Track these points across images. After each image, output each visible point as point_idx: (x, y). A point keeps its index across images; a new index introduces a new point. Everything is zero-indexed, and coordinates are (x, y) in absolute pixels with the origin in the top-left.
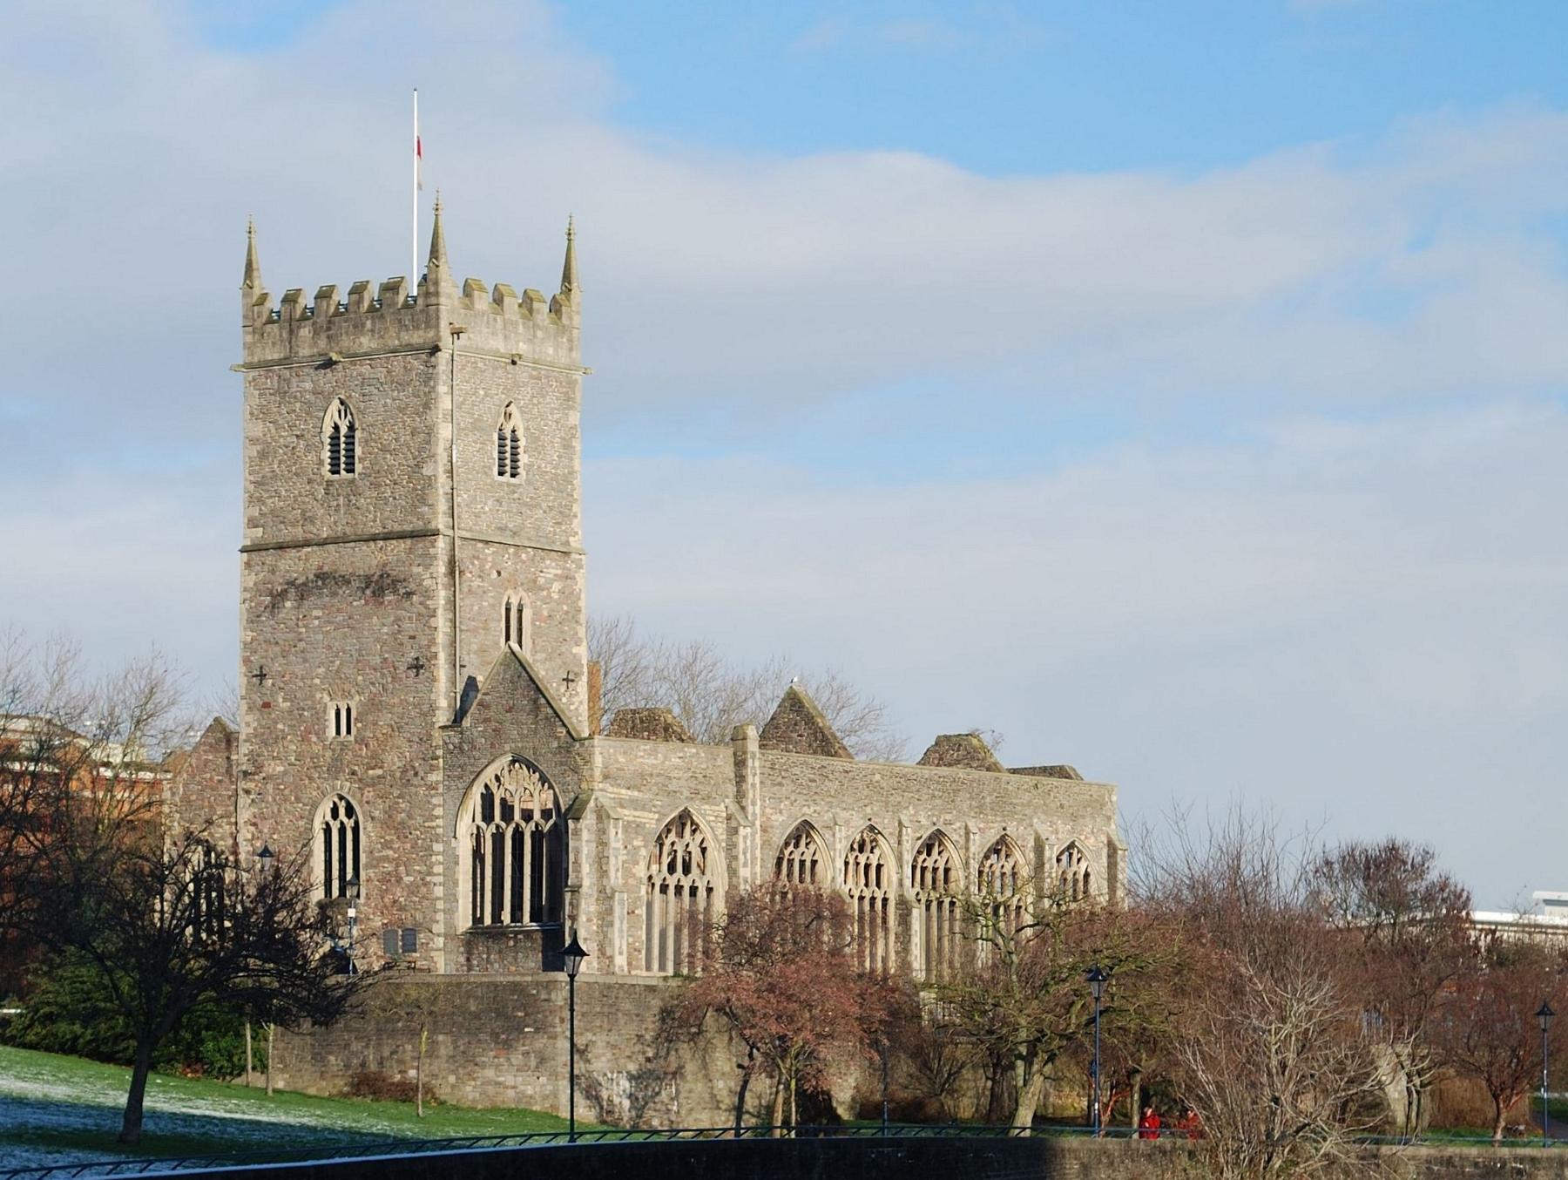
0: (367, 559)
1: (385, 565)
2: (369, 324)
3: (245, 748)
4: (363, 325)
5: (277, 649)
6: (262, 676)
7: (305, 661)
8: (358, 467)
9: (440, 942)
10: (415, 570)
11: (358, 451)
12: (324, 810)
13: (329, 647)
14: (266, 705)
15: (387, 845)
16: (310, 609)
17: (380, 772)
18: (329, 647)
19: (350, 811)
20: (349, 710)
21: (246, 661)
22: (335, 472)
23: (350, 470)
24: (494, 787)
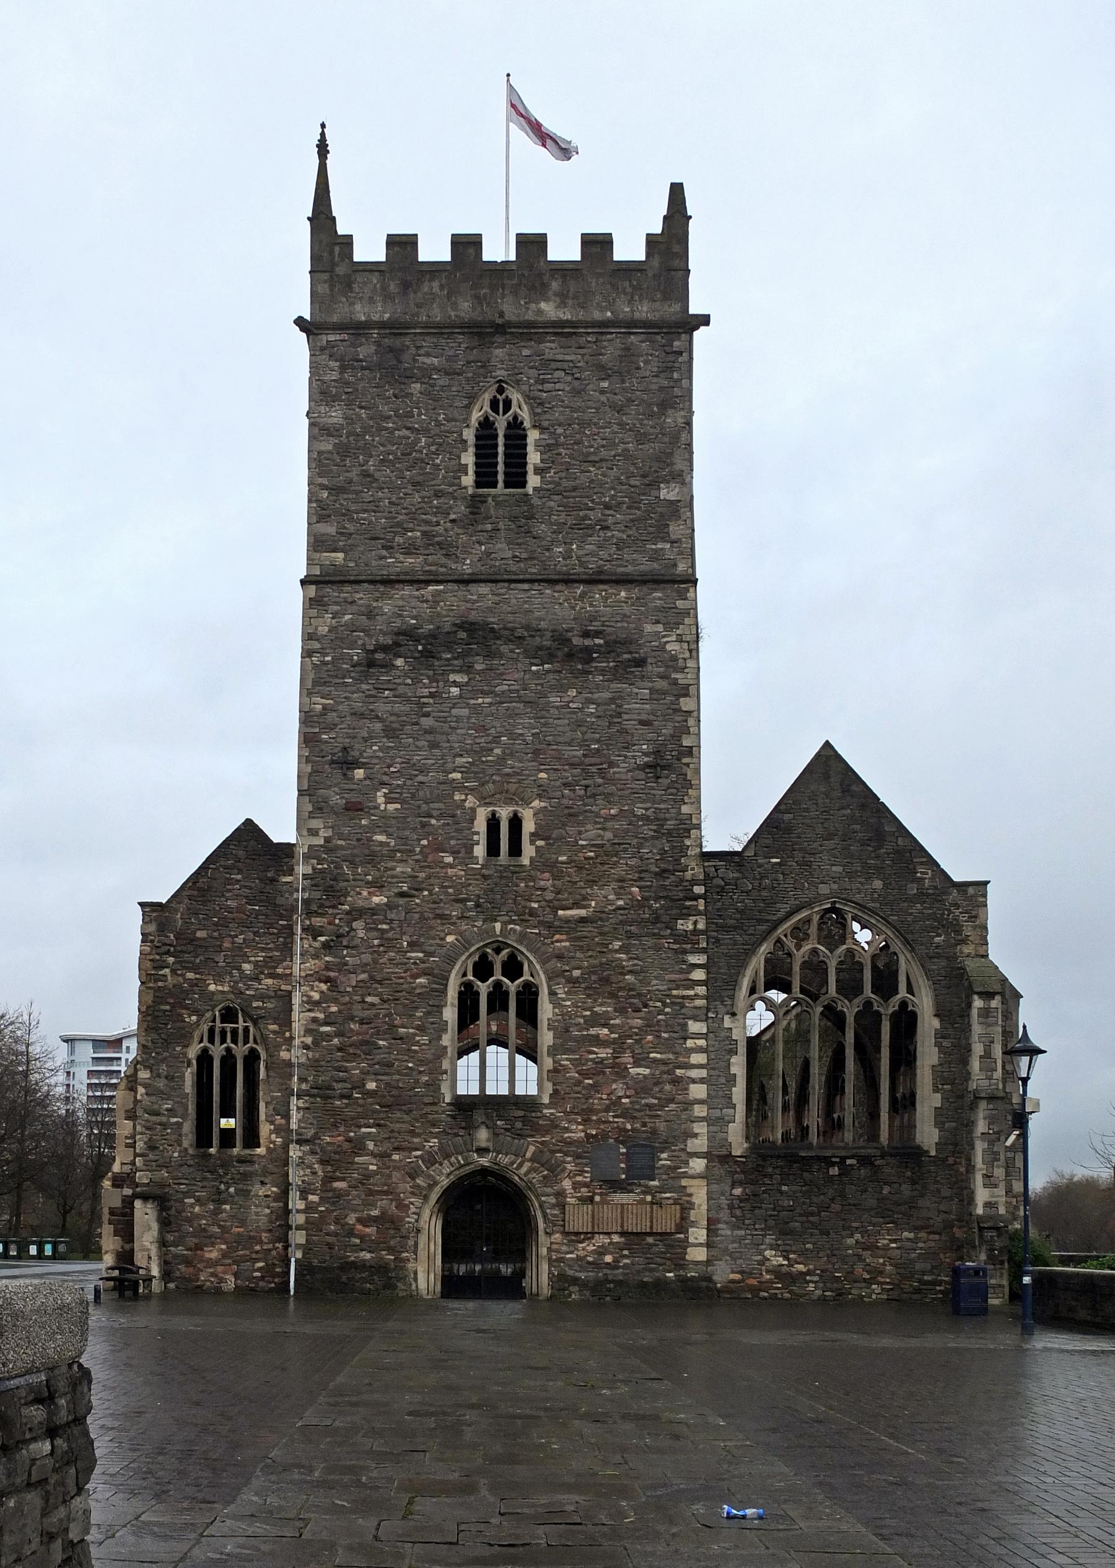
0: (554, 608)
1: (593, 619)
2: (555, 285)
3: (301, 869)
4: (545, 286)
5: (378, 726)
6: (347, 763)
7: (434, 745)
8: (533, 481)
9: (698, 1165)
10: (649, 628)
11: (534, 457)
12: (465, 963)
13: (482, 729)
14: (354, 808)
15: (597, 1020)
16: (445, 673)
17: (582, 912)
18: (482, 729)
19: (513, 968)
20: (516, 823)
21: (308, 740)
22: (485, 477)
23: (516, 478)
24: (790, 943)
